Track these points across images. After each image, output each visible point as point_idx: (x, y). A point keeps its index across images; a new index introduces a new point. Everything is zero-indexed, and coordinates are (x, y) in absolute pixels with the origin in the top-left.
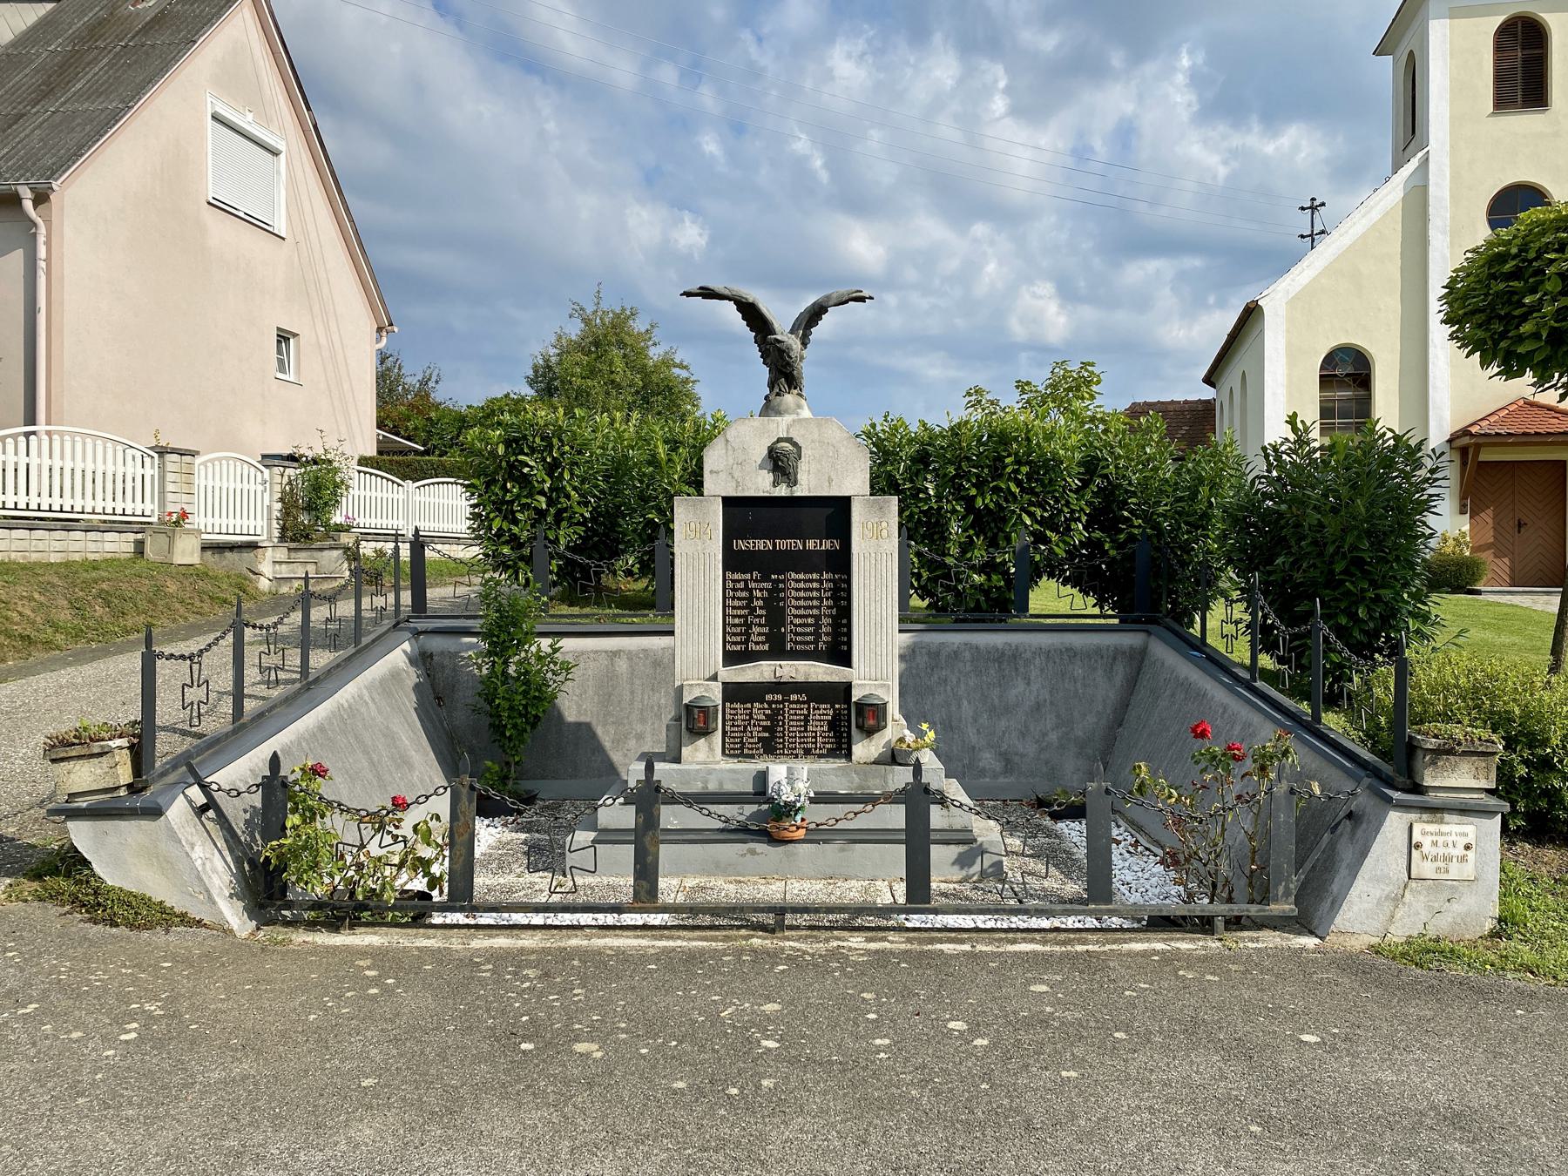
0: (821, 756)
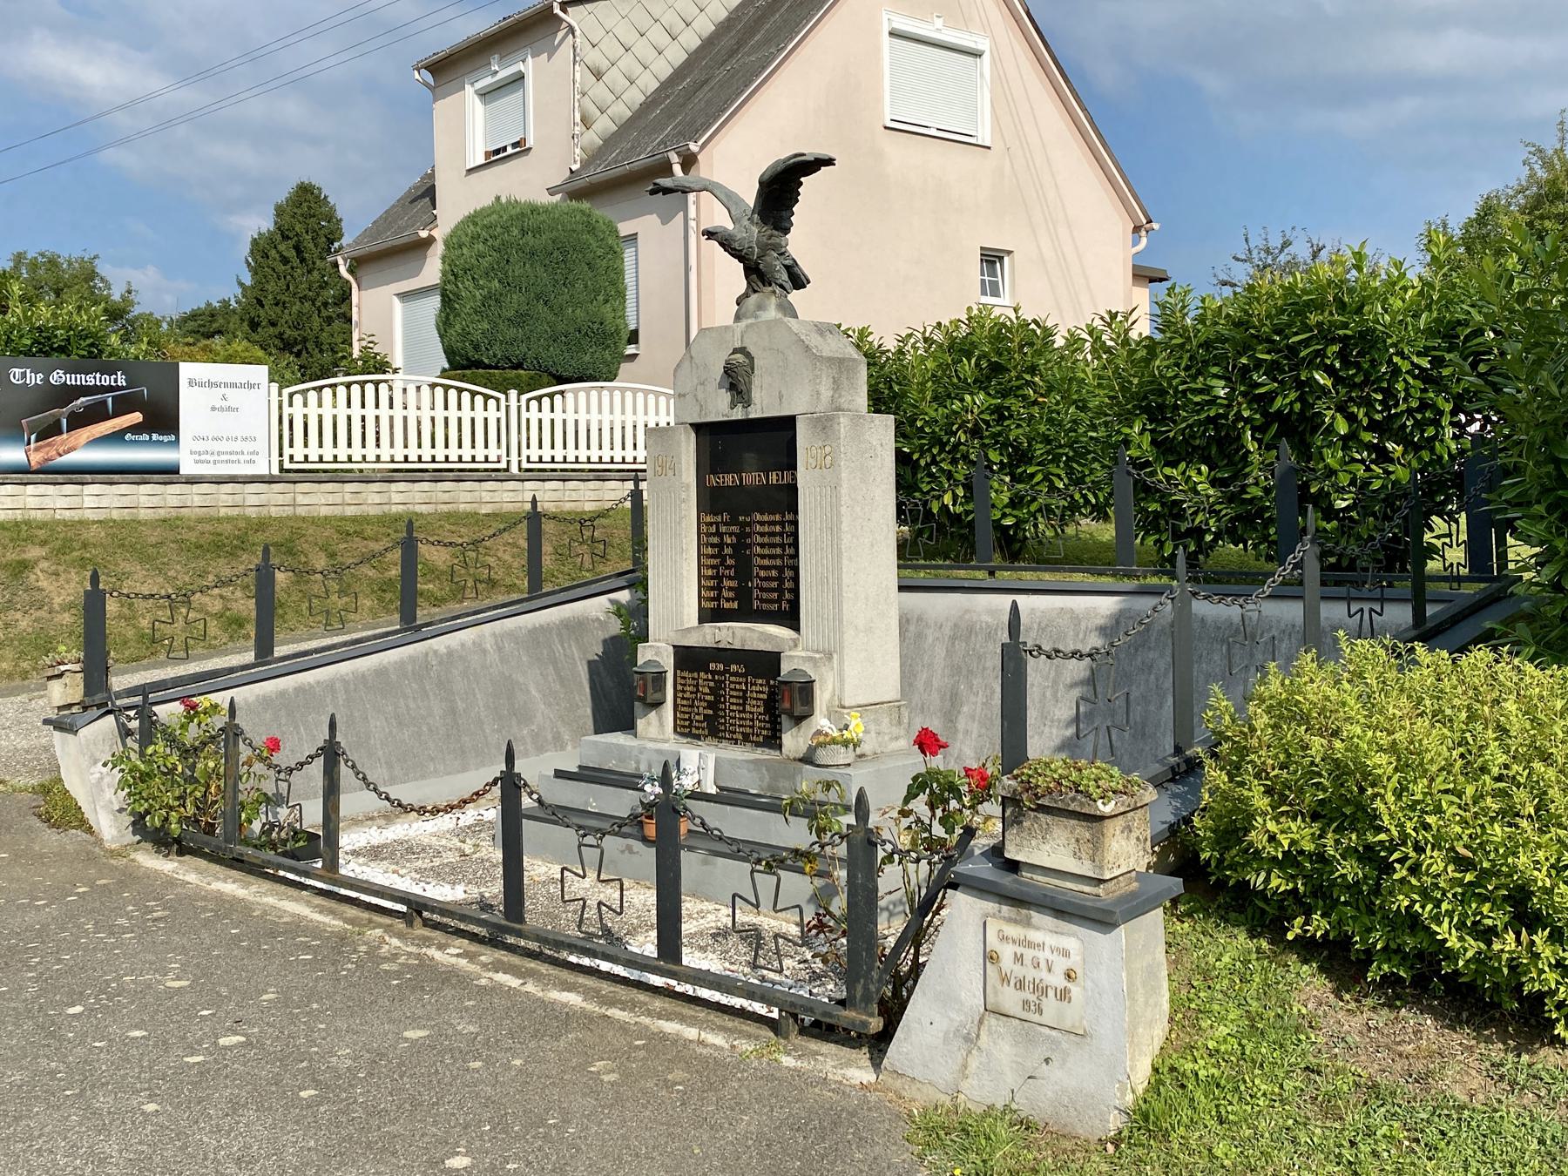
0: (758, 745)
